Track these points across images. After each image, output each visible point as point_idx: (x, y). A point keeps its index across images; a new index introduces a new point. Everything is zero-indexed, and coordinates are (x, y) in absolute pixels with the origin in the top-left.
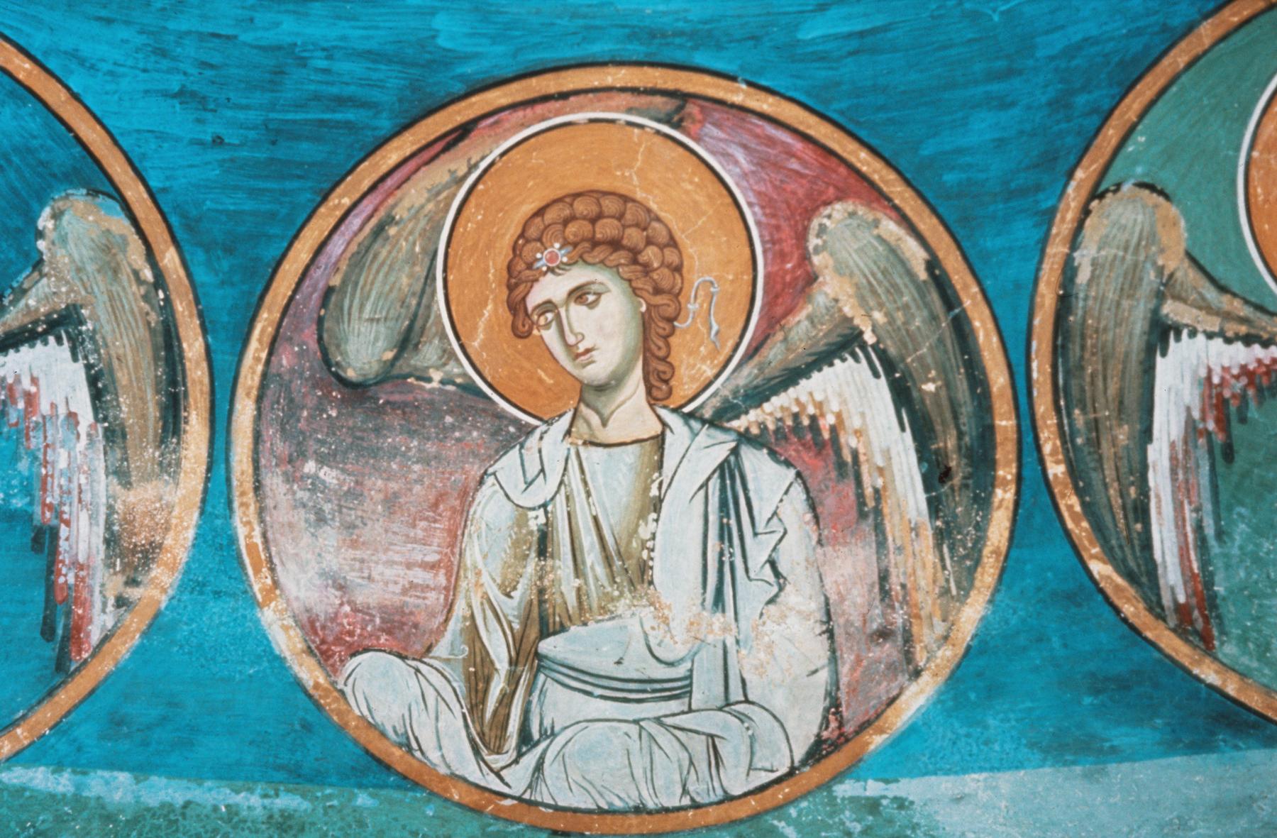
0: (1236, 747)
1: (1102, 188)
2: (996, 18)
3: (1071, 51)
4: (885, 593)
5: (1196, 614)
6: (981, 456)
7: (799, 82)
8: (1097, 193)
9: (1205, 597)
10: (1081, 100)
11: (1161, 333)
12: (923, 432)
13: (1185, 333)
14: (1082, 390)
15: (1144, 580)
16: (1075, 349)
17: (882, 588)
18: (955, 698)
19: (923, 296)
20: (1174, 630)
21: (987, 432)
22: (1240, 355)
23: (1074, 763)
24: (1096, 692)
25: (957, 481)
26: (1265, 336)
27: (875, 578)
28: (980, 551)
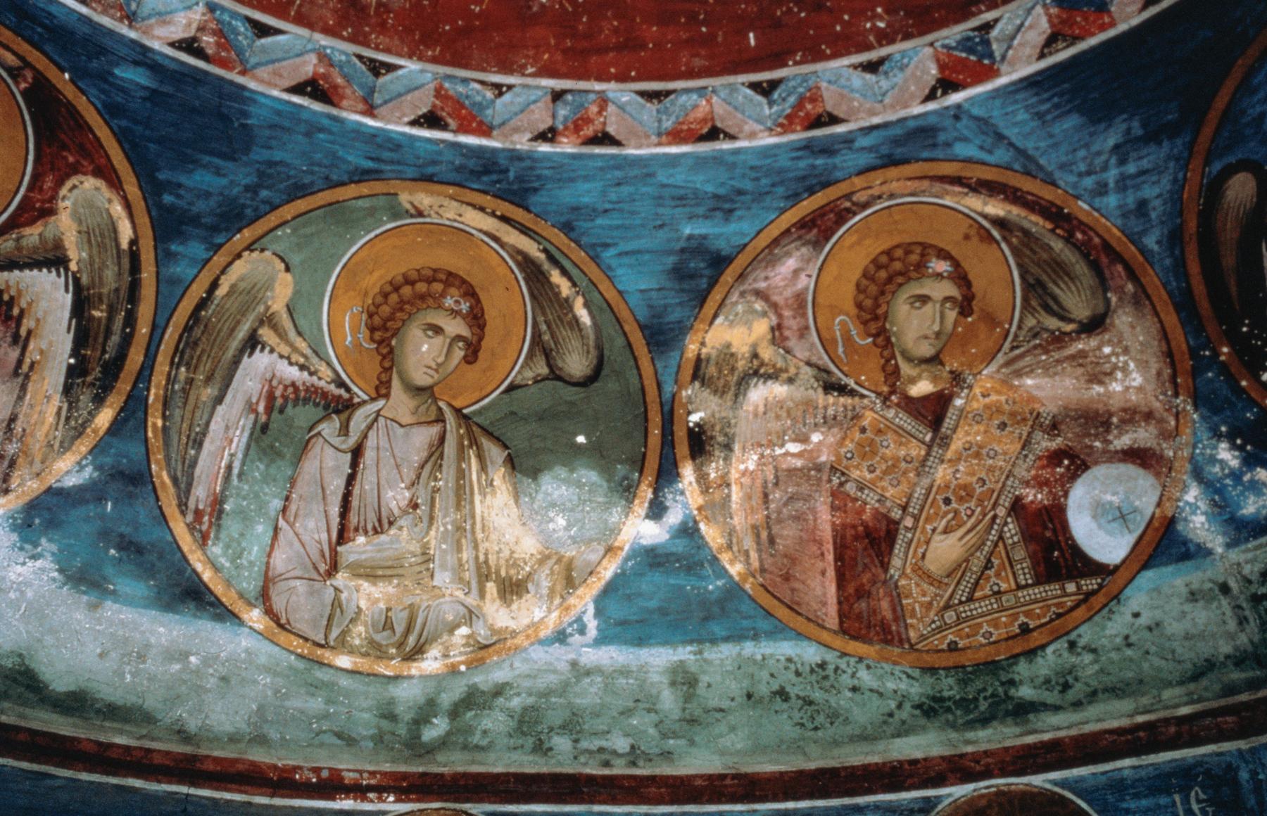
0: (195, 616)
1: (256, 246)
2: (236, 125)
3: (271, 164)
4: (9, 429)
5: (206, 518)
6: (113, 369)
7: (103, 97)
8: (249, 248)
9: (217, 503)
10: (264, 193)
11: (253, 343)
12: (83, 337)
13: (268, 349)
14: (192, 358)
15: (183, 486)
16: (197, 332)
17: (9, 425)
18: (24, 519)
19: (119, 257)
20: (188, 525)
21: (121, 356)
22: (293, 373)
23: (84, 593)
24: (120, 548)
25: (89, 379)
26: (312, 369)
27: (7, 417)
28: (85, 428)
